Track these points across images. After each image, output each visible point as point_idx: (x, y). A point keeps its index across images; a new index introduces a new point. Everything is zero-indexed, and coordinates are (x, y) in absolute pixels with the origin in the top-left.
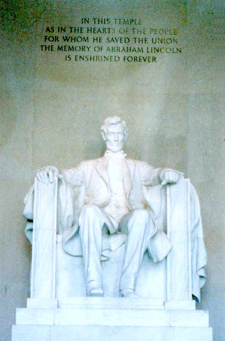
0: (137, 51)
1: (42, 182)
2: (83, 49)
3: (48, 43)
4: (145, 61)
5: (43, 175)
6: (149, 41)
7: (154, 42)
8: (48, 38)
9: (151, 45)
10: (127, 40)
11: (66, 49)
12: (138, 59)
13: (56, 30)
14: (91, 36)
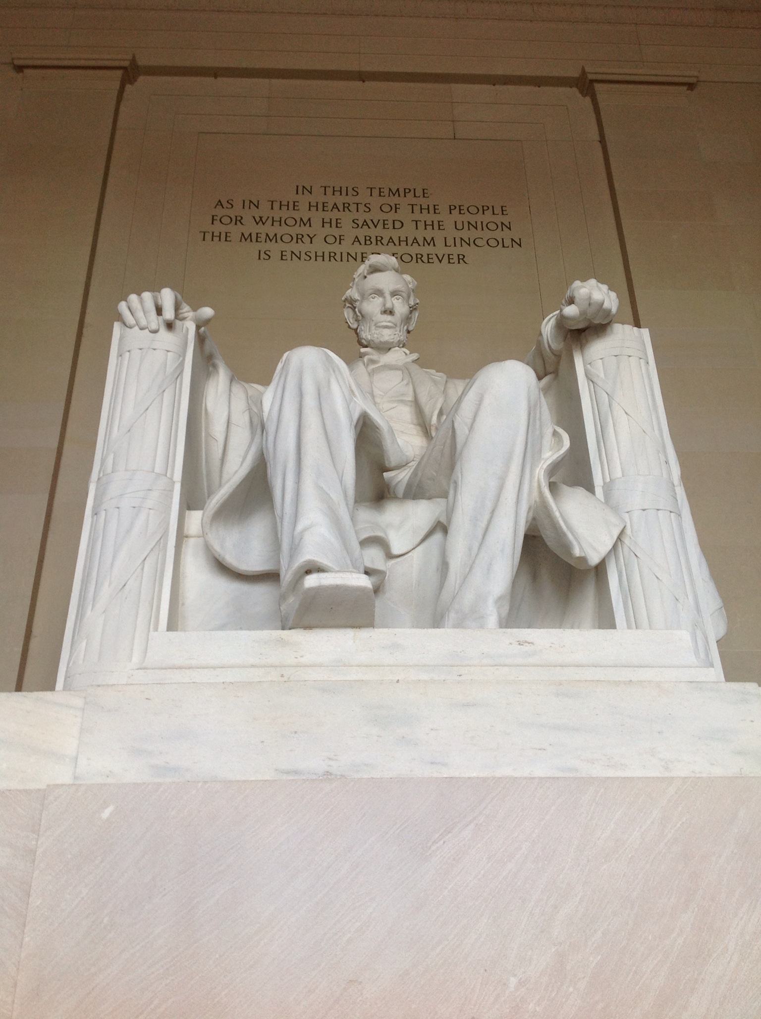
0: (421, 244)
1: (137, 328)
2: (299, 238)
3: (218, 228)
4: (440, 261)
5: (141, 301)
6: (449, 224)
7: (459, 226)
8: (218, 219)
9: (450, 232)
10: (398, 225)
11: (259, 240)
12: (425, 259)
13: (238, 204)
14: (317, 217)
